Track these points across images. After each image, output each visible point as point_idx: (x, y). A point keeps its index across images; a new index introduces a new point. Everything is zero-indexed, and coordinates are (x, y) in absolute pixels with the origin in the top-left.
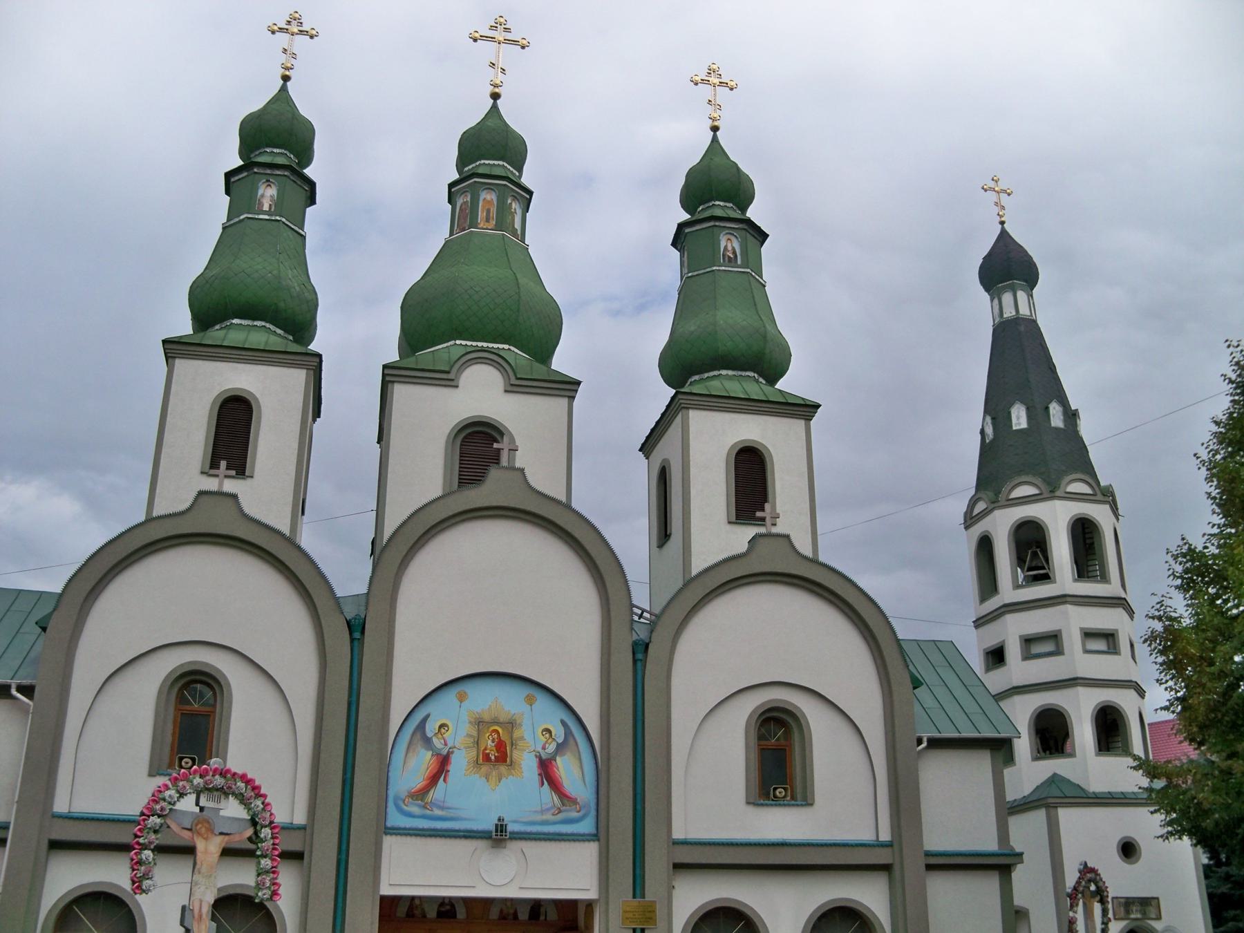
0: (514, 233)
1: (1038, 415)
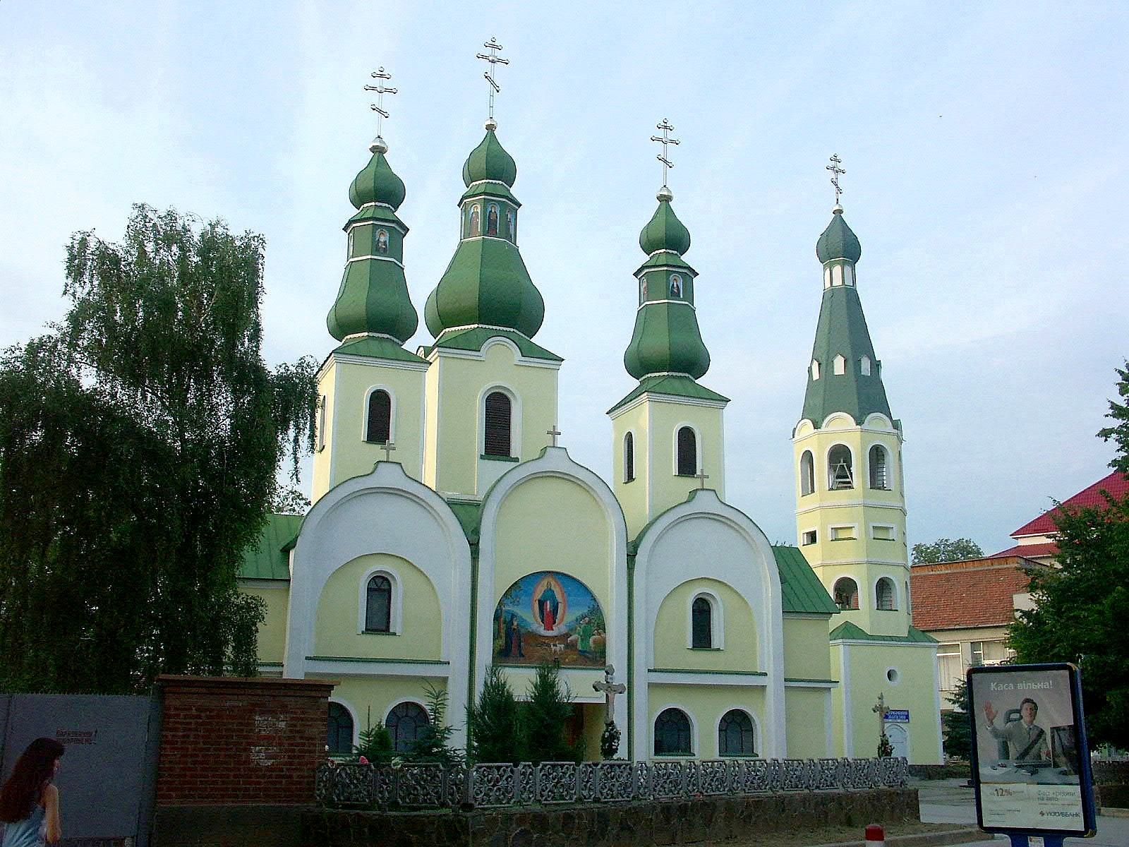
1: (853, 363)
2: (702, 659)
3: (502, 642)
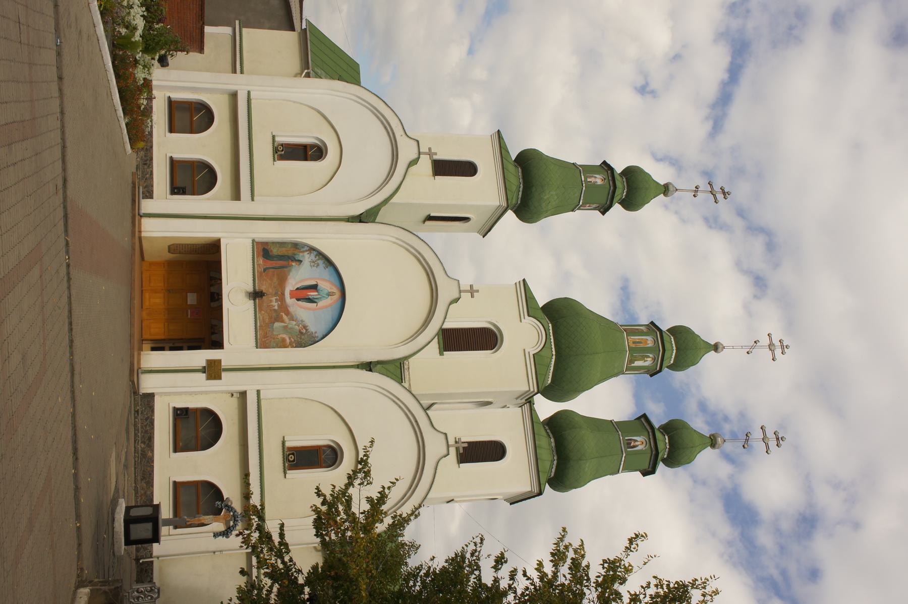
0: (631, 361)
2: (274, 458)
3: (275, 251)
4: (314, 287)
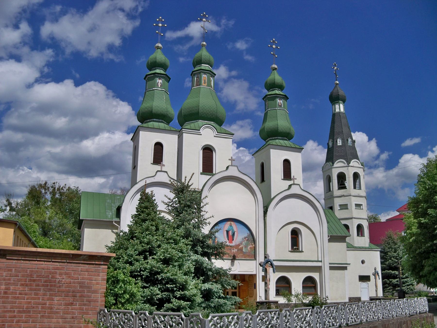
1: (345, 141)
4: (228, 232)
